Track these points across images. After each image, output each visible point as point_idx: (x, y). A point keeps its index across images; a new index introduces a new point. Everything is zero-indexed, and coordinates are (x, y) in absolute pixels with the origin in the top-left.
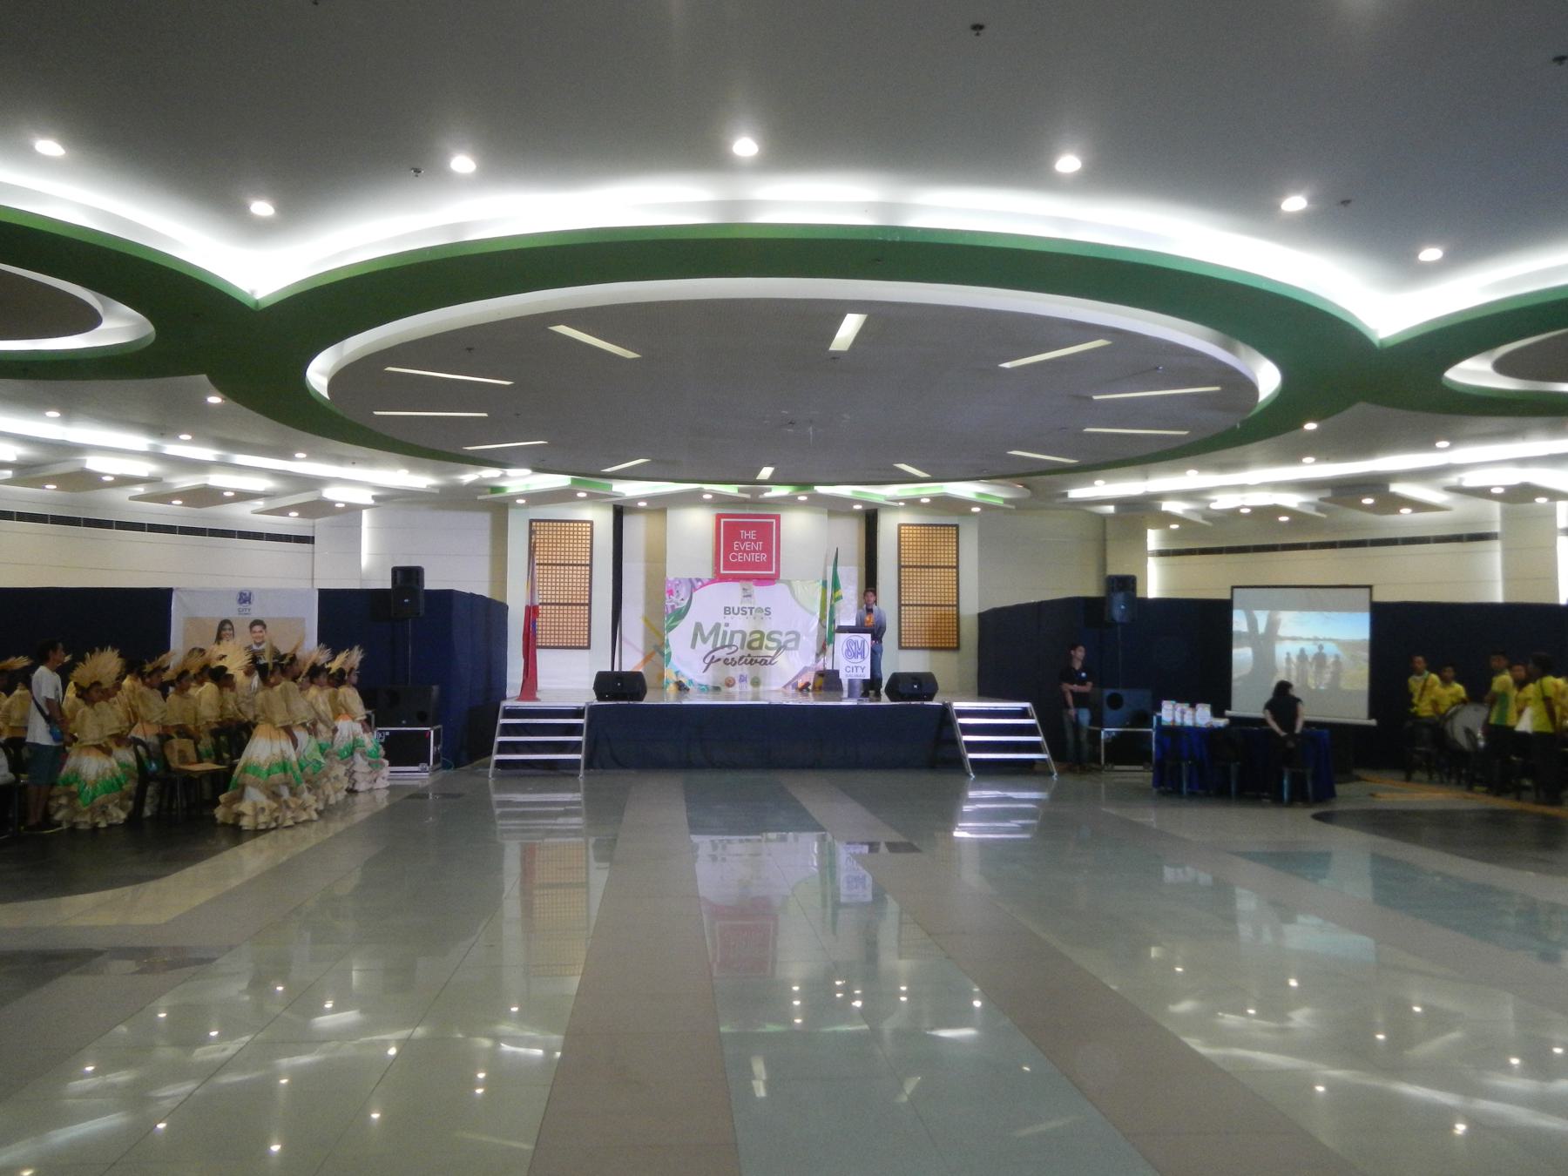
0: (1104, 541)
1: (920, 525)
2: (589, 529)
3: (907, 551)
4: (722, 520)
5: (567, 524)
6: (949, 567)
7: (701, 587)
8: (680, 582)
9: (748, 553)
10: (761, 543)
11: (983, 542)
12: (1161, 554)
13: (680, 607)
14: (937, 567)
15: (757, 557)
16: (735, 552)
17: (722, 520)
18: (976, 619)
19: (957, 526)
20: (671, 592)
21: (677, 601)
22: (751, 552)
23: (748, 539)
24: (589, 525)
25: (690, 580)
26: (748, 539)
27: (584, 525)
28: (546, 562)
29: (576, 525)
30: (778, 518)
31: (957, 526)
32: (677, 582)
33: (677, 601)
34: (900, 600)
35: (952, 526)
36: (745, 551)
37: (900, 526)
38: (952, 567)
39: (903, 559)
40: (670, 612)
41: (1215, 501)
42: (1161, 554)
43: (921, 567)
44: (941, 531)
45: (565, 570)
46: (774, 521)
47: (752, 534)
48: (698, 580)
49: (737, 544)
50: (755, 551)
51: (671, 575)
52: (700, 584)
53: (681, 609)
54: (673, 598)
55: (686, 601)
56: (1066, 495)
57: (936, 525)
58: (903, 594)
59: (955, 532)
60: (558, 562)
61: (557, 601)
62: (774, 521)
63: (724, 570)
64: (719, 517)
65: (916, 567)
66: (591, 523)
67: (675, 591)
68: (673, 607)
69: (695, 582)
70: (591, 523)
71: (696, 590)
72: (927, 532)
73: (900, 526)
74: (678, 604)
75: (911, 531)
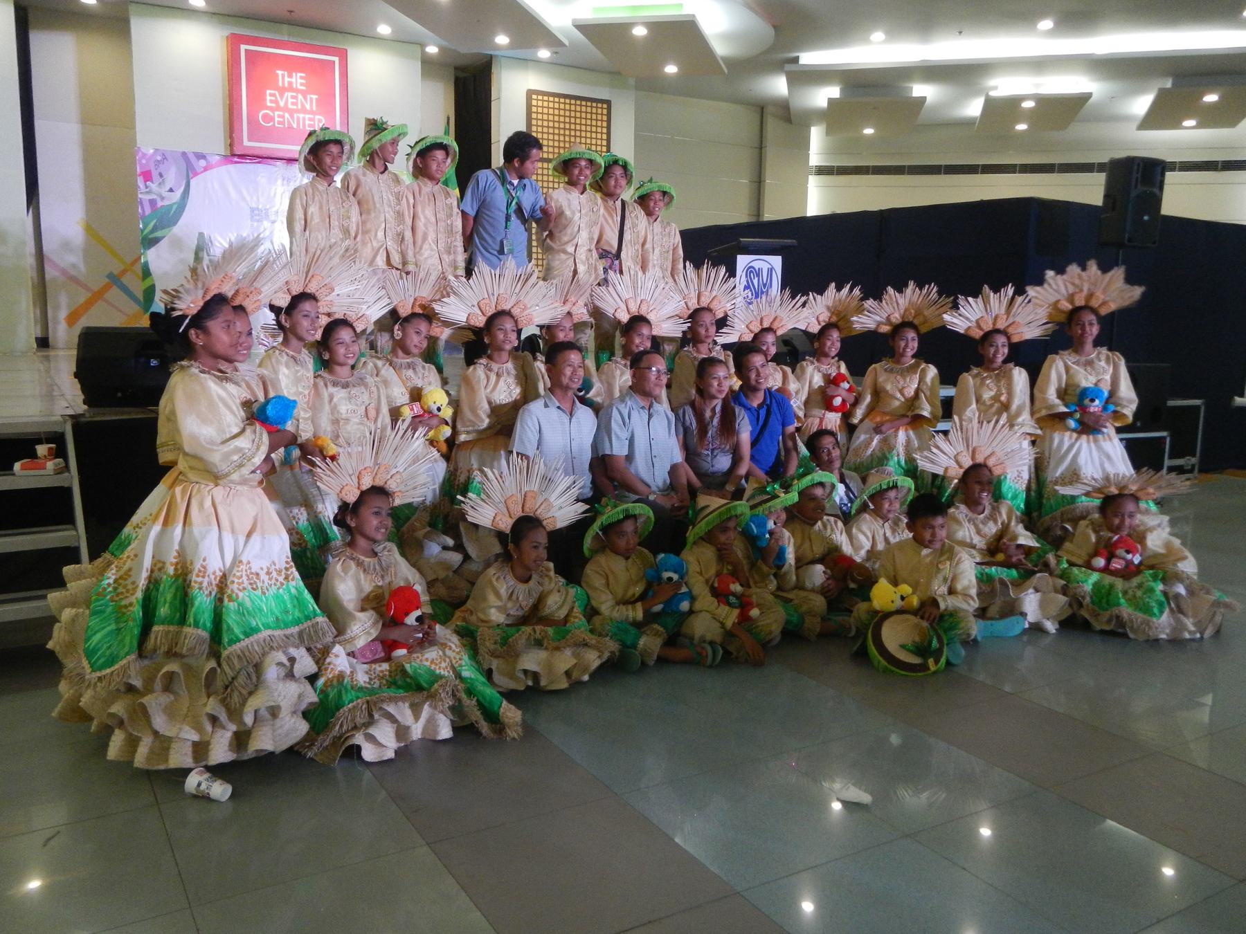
0: (761, 148)
1: (565, 96)
7: (206, 169)
8: (165, 158)
10: (314, 97)
12: (821, 171)
13: (166, 203)
15: (307, 122)
16: (267, 108)
17: (243, 47)
19: (608, 103)
20: (147, 176)
21: (163, 191)
22: (298, 111)
23: (290, 88)
25: (184, 154)
30: (343, 56)
31: (608, 103)
32: (159, 158)
33: (163, 191)
35: (602, 101)
36: (285, 109)
37: (530, 93)
40: (148, 211)
41: (995, 88)
42: (821, 171)
44: (586, 107)
46: (336, 59)
47: (298, 80)
48: (200, 156)
49: (271, 95)
50: (304, 111)
51: (148, 141)
52: (203, 163)
53: (171, 206)
54: (153, 186)
55: (177, 195)
56: (796, 60)
59: (605, 112)
63: (250, 140)
64: (234, 42)
67: (155, 174)
68: (152, 203)
69: (192, 157)
71: (196, 174)
73: (530, 93)
74: (163, 198)
75: (546, 104)
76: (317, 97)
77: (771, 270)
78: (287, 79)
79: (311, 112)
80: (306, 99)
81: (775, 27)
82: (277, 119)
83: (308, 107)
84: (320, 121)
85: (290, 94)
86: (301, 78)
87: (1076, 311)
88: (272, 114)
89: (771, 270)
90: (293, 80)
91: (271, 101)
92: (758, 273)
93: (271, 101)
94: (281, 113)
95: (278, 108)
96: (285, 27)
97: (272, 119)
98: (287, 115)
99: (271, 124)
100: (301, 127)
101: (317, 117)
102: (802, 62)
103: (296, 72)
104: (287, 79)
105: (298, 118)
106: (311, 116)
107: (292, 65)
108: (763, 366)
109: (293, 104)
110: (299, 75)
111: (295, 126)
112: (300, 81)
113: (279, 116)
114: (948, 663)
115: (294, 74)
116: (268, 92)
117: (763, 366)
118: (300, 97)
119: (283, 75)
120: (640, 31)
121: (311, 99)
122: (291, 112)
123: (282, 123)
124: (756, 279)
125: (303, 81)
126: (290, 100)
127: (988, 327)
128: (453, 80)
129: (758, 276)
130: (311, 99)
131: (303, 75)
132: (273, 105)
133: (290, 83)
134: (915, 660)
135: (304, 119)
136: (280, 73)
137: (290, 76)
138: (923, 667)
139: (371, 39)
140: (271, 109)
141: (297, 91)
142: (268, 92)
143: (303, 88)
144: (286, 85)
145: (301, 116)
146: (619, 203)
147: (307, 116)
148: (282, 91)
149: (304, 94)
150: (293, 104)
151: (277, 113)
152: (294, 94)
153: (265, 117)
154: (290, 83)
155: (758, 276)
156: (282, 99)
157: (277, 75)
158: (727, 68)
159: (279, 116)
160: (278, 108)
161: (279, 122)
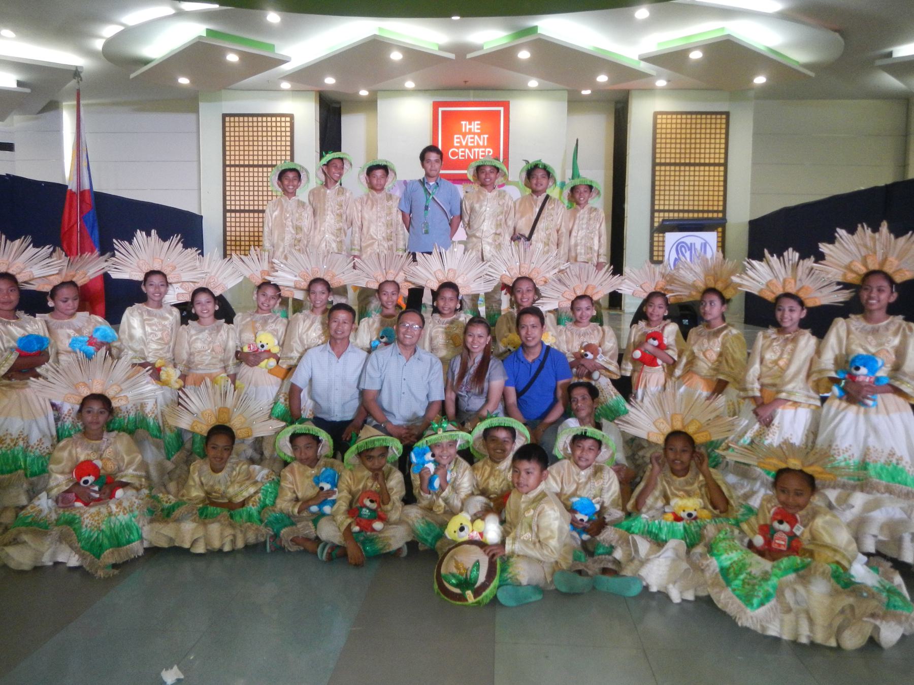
1: (682, 113)
2: (288, 124)
3: (663, 146)
4: (441, 109)
5: (269, 119)
6: (714, 165)
10: (486, 136)
11: (760, 136)
14: (700, 165)
15: (481, 154)
17: (441, 109)
18: (747, 228)
19: (727, 114)
22: (475, 147)
23: (470, 133)
24: (288, 119)
26: (470, 133)
27: (283, 119)
28: (242, 163)
29: (274, 119)
30: (506, 105)
31: (727, 114)
34: (653, 204)
35: (721, 113)
36: (466, 146)
37: (656, 114)
38: (719, 165)
39: (658, 156)
43: (680, 164)
45: (263, 172)
46: (502, 109)
47: (475, 126)
49: (457, 138)
50: (478, 146)
56: (890, 54)
57: (707, 113)
58: (657, 197)
59: (724, 121)
60: (256, 163)
61: (256, 208)
62: (502, 109)
64: (436, 105)
65: (675, 164)
66: (292, 116)
70: (292, 116)
72: (689, 121)
77: (704, 245)
78: (468, 127)
80: (480, 138)
81: (836, 31)
82: (460, 154)
83: (481, 143)
85: (470, 136)
86: (478, 124)
87: (871, 273)
89: (704, 245)
90: (472, 127)
91: (457, 142)
92: (691, 248)
93: (457, 142)
94: (463, 150)
95: (461, 146)
96: (472, 92)
97: (457, 154)
98: (467, 150)
101: (487, 150)
102: (895, 55)
103: (475, 120)
104: (468, 127)
105: (475, 152)
106: (483, 149)
107: (470, 117)
108: (533, 326)
109: (471, 142)
110: (476, 122)
111: (472, 157)
112: (476, 127)
113: (462, 152)
114: (495, 600)
116: (456, 136)
117: (533, 326)
118: (476, 137)
119: (466, 125)
120: (696, 55)
121: (484, 138)
122: (470, 149)
123: (464, 156)
124: (688, 253)
125: (479, 127)
126: (470, 140)
127: (779, 291)
128: (614, 110)
129: (690, 249)
130: (484, 138)
131: (479, 122)
132: (458, 145)
133: (470, 129)
134: (457, 591)
135: (478, 152)
136: (463, 123)
137: (470, 124)
138: (462, 598)
139: (525, 91)
140: (458, 148)
141: (474, 134)
142: (456, 136)
143: (479, 131)
144: (467, 131)
145: (476, 150)
146: (541, 198)
147: (481, 150)
148: (464, 135)
149: (479, 135)
150: (471, 142)
151: (461, 150)
152: (472, 136)
153: (454, 154)
154: (470, 129)
155: (690, 249)
156: (464, 138)
157: (462, 125)
158: (811, 71)
159: (462, 152)
160: (461, 146)
161: (462, 156)
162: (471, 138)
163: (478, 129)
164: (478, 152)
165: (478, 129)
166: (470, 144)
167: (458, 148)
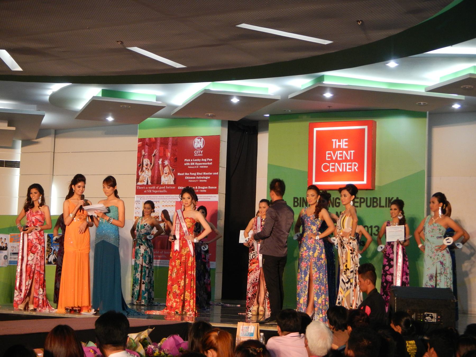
9: (339, 162)
10: (352, 151)
15: (348, 167)
22: (343, 161)
23: (339, 148)
36: (336, 161)
47: (343, 143)
49: (329, 154)
50: (346, 160)
76: (354, 151)
79: (351, 161)
82: (331, 167)
83: (349, 158)
84: (355, 165)
85: (339, 152)
86: (346, 141)
88: (328, 165)
90: (341, 143)
91: (328, 158)
93: (328, 158)
95: (332, 161)
99: (328, 170)
100: (344, 170)
101: (353, 163)
104: (337, 144)
107: (339, 135)
110: (344, 140)
112: (344, 143)
115: (342, 140)
116: (327, 152)
119: (336, 142)
121: (351, 153)
125: (347, 143)
130: (351, 153)
133: (339, 146)
135: (346, 165)
136: (334, 140)
137: (339, 142)
141: (343, 149)
142: (327, 152)
145: (344, 163)
150: (340, 157)
151: (331, 164)
154: (339, 146)
159: (333, 165)
161: (332, 169)
162: (340, 153)
163: (346, 145)
164: (346, 165)
165: (346, 145)
166: (338, 159)
167: (329, 162)
